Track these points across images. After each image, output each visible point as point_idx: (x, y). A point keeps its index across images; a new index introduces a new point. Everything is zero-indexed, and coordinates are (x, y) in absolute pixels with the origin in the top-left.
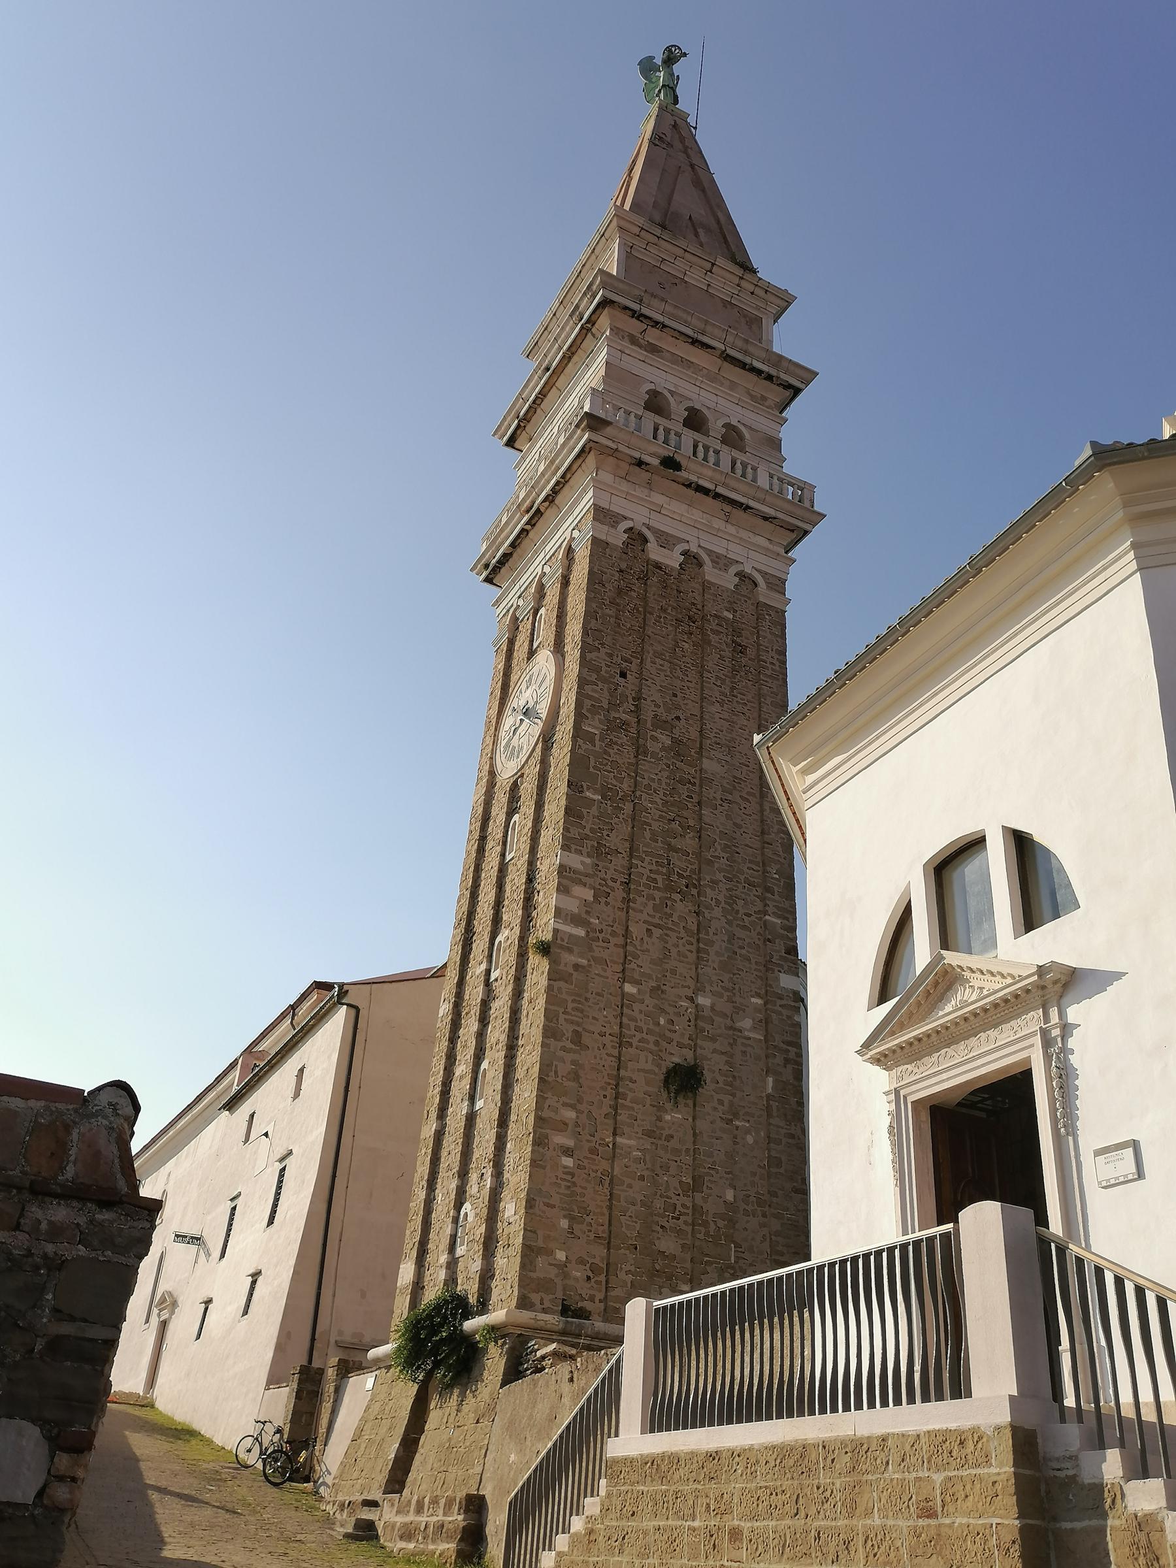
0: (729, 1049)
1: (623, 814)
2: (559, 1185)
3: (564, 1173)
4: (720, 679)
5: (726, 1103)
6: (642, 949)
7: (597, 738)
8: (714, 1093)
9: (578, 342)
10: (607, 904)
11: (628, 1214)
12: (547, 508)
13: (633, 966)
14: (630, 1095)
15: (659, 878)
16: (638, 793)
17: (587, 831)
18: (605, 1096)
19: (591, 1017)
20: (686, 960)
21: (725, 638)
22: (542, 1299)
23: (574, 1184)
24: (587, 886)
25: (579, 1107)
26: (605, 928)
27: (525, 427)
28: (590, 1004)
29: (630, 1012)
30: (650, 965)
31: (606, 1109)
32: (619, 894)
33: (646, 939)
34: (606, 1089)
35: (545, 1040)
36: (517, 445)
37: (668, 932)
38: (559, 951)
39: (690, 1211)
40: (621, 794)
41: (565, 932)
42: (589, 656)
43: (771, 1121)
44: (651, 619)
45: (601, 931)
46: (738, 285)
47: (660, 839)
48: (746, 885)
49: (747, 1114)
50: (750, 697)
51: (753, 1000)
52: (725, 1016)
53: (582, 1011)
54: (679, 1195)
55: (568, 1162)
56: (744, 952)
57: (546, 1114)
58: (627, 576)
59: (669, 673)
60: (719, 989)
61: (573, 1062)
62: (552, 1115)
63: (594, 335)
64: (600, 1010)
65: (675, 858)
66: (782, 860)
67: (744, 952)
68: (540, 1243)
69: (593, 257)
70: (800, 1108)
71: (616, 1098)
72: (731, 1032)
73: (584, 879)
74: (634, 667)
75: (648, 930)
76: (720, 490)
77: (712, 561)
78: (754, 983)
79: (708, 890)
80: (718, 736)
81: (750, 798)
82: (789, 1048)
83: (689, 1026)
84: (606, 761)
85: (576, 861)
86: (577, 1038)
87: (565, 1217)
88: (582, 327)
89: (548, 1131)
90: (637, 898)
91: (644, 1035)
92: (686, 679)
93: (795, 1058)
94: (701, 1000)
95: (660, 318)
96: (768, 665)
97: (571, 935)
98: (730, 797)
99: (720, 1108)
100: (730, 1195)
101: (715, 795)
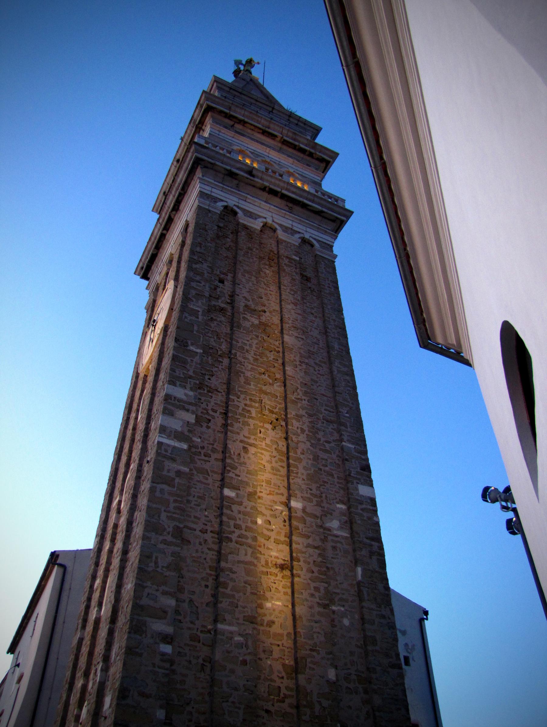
1: (222, 365)
3: (162, 660)
4: (293, 291)
6: (239, 462)
7: (200, 313)
11: (231, 699)
12: (175, 215)
13: (231, 474)
14: (231, 584)
16: (233, 351)
17: (191, 373)
18: (206, 586)
19: (192, 517)
20: (278, 473)
21: (294, 270)
23: (173, 672)
24: (190, 411)
26: (205, 444)
28: (192, 505)
29: (228, 512)
31: (207, 598)
32: (219, 421)
34: (207, 580)
35: (146, 533)
37: (263, 451)
39: (294, 693)
40: (220, 353)
41: (169, 446)
42: (194, 266)
43: (364, 604)
44: (241, 253)
45: (203, 448)
48: (325, 422)
49: (341, 599)
50: (316, 305)
51: (339, 506)
52: (316, 517)
53: (183, 510)
54: (283, 678)
55: (167, 649)
56: (327, 469)
57: (145, 601)
59: (256, 283)
60: (309, 496)
61: (173, 554)
62: (151, 603)
64: (201, 510)
66: (351, 405)
67: (327, 469)
70: (387, 592)
71: (217, 588)
72: (321, 530)
73: (187, 406)
76: (284, 192)
78: (337, 492)
79: (294, 422)
80: (294, 323)
81: (323, 365)
82: (373, 543)
83: (285, 526)
84: (207, 331)
85: (179, 393)
86: (178, 533)
88: (197, 127)
89: (148, 619)
90: (234, 423)
91: (243, 532)
92: (268, 289)
93: (378, 551)
95: (243, 118)
96: (326, 287)
97: (174, 447)
98: (306, 361)
99: (317, 594)
100: (332, 674)
101: (295, 358)
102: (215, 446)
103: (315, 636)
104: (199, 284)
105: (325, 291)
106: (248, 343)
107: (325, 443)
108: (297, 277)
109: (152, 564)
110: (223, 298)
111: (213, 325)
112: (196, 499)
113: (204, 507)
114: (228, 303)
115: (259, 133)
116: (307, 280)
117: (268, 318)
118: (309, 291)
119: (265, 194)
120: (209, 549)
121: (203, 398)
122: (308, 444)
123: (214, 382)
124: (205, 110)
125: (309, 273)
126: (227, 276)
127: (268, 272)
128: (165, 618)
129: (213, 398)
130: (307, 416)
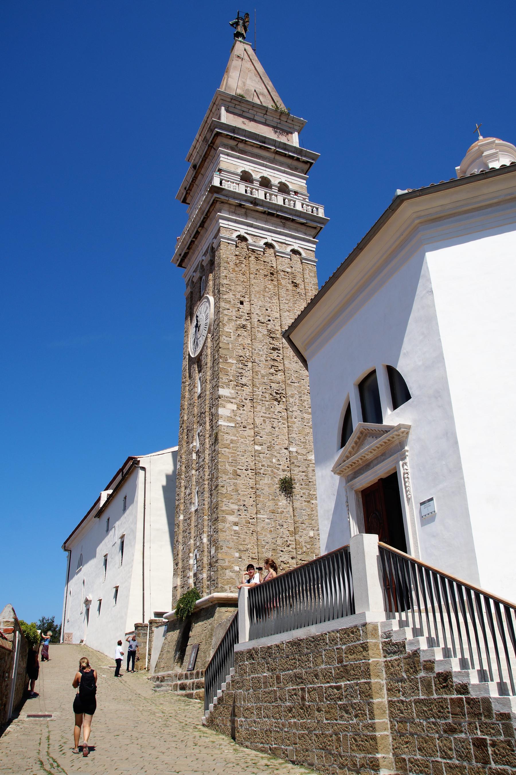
0: (306, 469)
2: (232, 538)
5: (307, 494)
7: (232, 334)
8: (300, 490)
9: (208, 152)
10: (244, 410)
11: (266, 547)
12: (201, 230)
13: (258, 437)
15: (267, 395)
17: (231, 378)
22: (230, 587)
25: (239, 503)
27: (189, 193)
29: (258, 458)
30: (267, 436)
33: (263, 424)
36: (188, 201)
37: (273, 420)
38: (223, 434)
39: (294, 543)
46: (280, 119)
47: (266, 378)
55: (236, 528)
58: (240, 257)
59: (263, 300)
62: (227, 508)
63: (214, 149)
65: (273, 385)
68: (227, 564)
69: (212, 113)
74: (247, 299)
75: (264, 420)
77: (279, 246)
87: (237, 552)
88: (209, 146)
89: (226, 515)
91: (266, 468)
94: (293, 449)
99: (304, 496)
102: (248, 421)
103: (303, 516)
104: (228, 311)
105: (309, 294)
106: (261, 349)
107: (308, 409)
108: (290, 288)
109: (225, 490)
110: (244, 317)
111: (240, 339)
112: (241, 453)
113: (246, 457)
114: (247, 320)
115: (257, 147)
116: (296, 286)
117: (272, 326)
118: (298, 296)
119: (265, 216)
120: (250, 478)
121: (239, 392)
122: (299, 411)
123: (244, 380)
124: (215, 135)
125: (298, 281)
126: (245, 297)
127: (270, 287)
128: (234, 515)
129: (245, 391)
130: (297, 393)
